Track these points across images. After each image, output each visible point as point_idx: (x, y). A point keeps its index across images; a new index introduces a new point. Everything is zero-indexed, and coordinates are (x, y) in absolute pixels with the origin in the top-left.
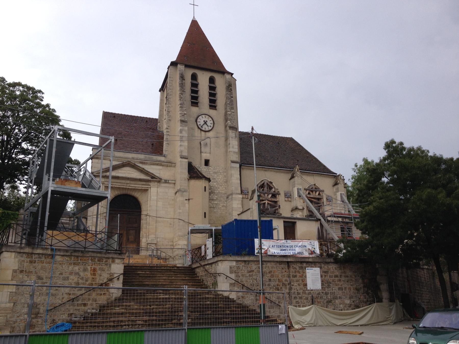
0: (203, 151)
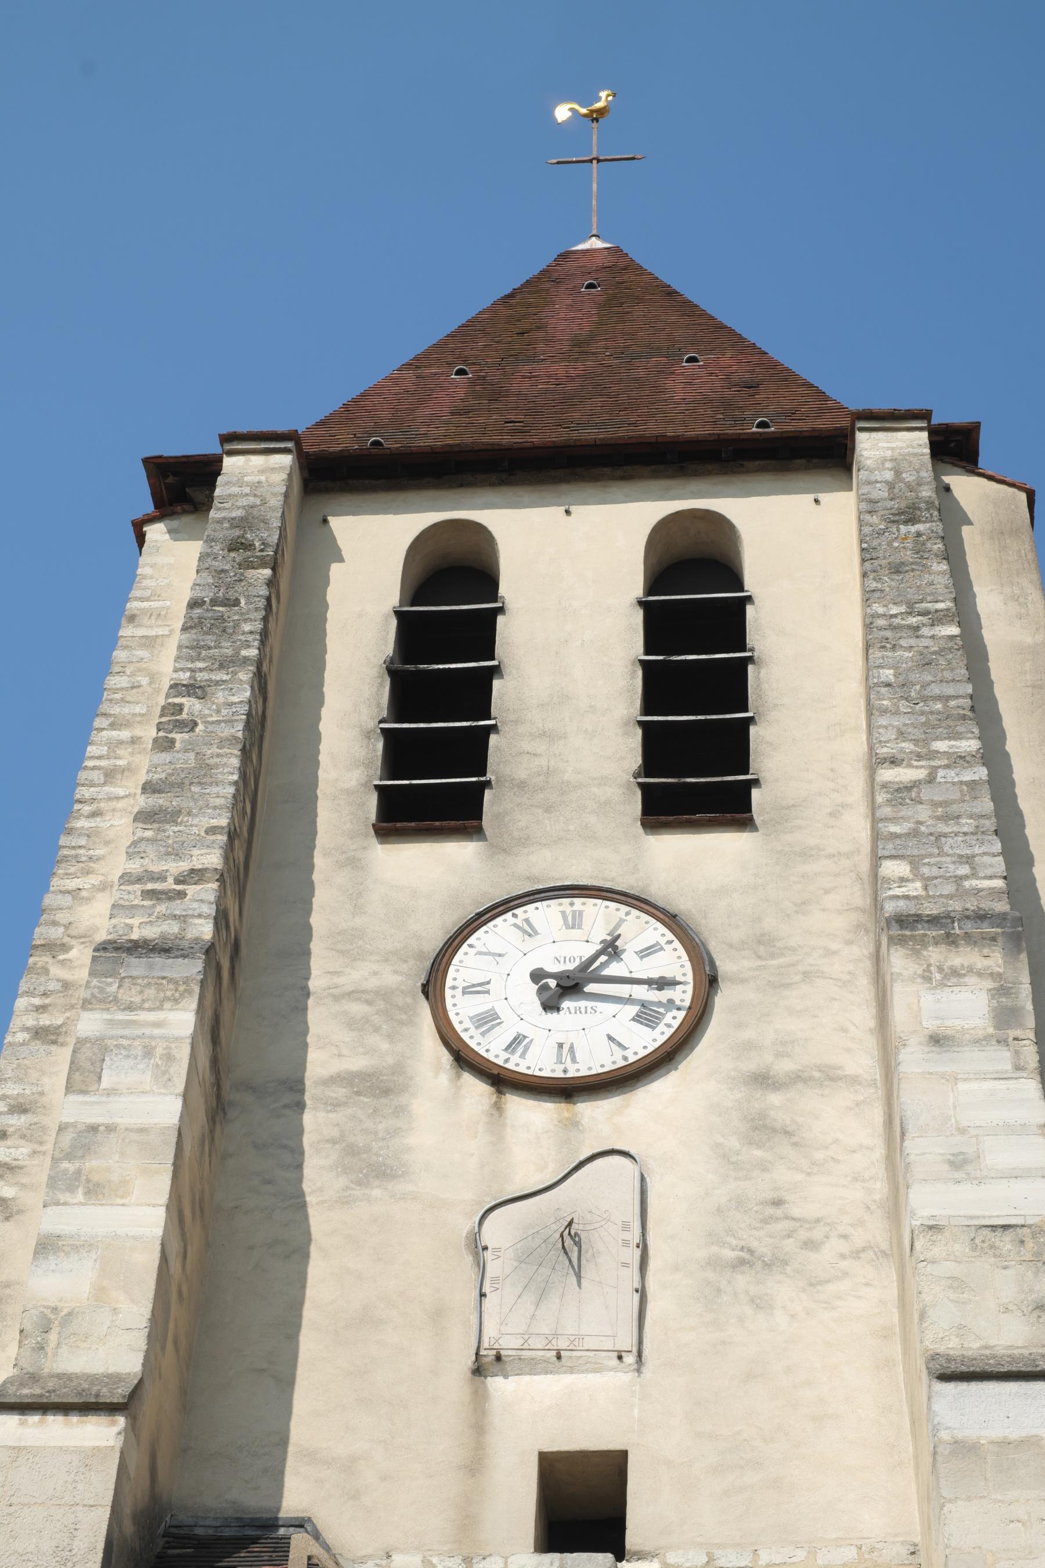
0: (509, 1344)
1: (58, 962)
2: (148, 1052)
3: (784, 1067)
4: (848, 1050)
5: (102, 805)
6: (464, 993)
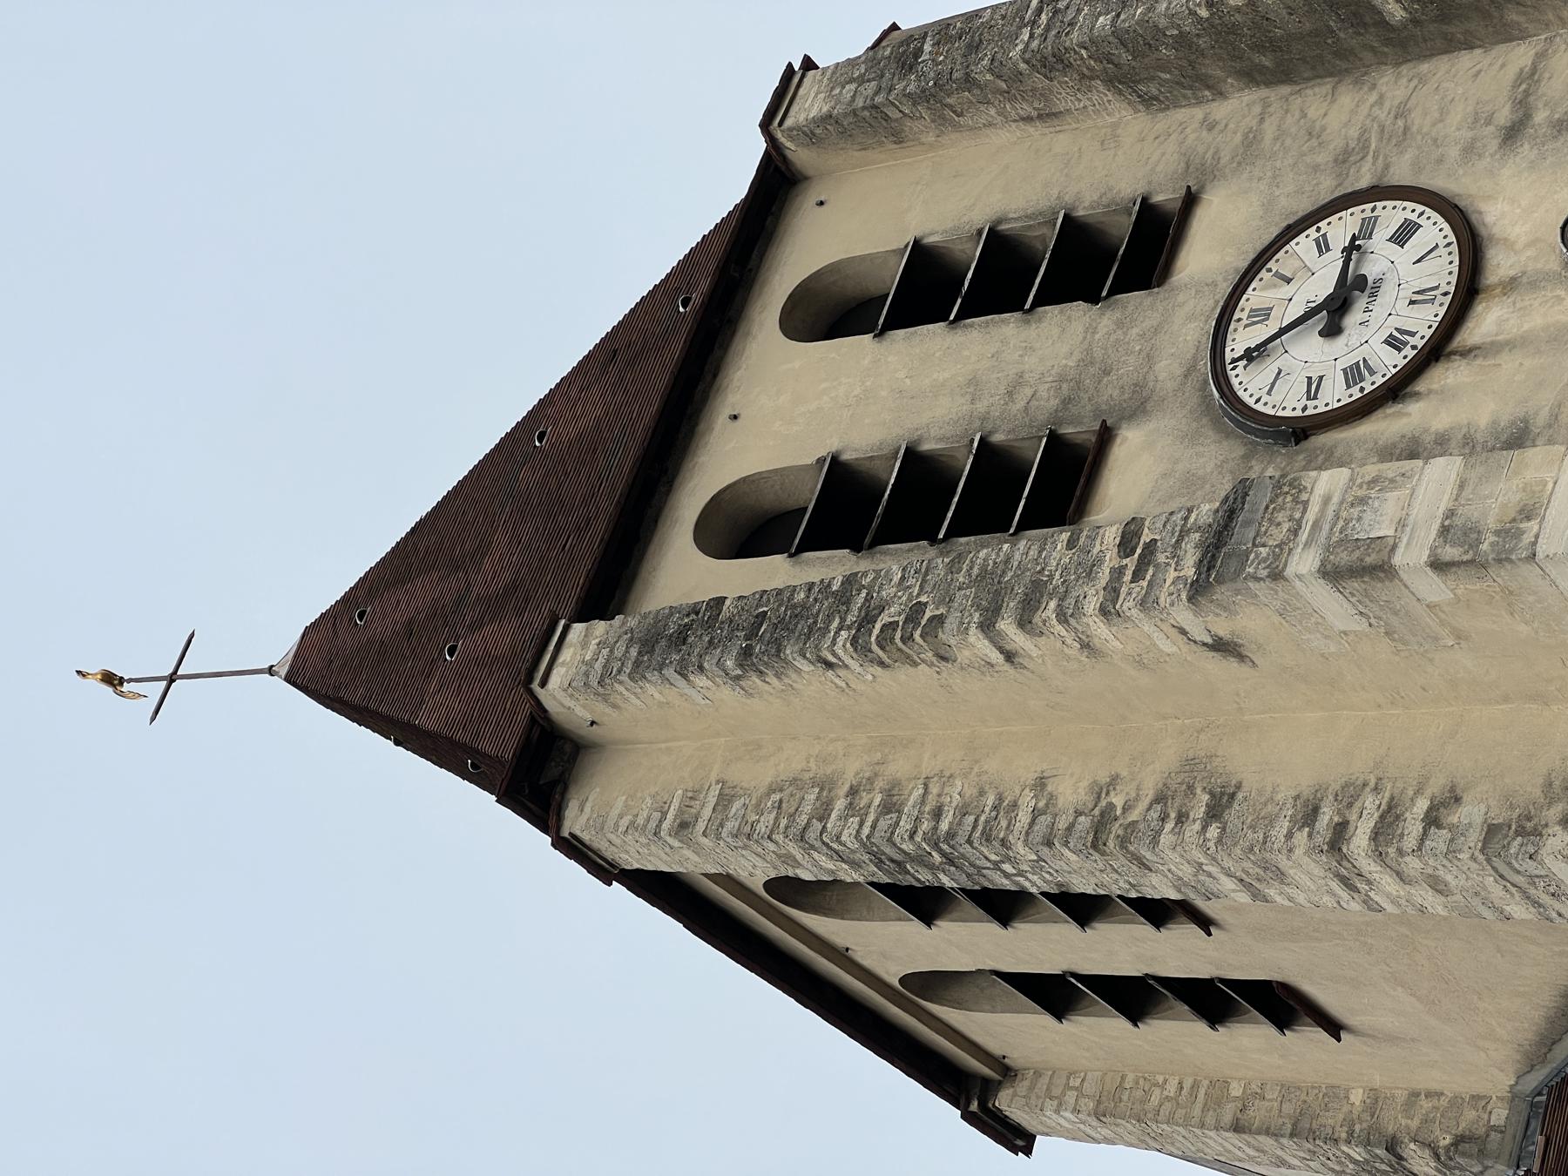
1: (1124, 813)
2: (1363, 501)
3: (1504, 116)
4: (1503, 66)
5: (927, 809)
6: (1315, 398)
